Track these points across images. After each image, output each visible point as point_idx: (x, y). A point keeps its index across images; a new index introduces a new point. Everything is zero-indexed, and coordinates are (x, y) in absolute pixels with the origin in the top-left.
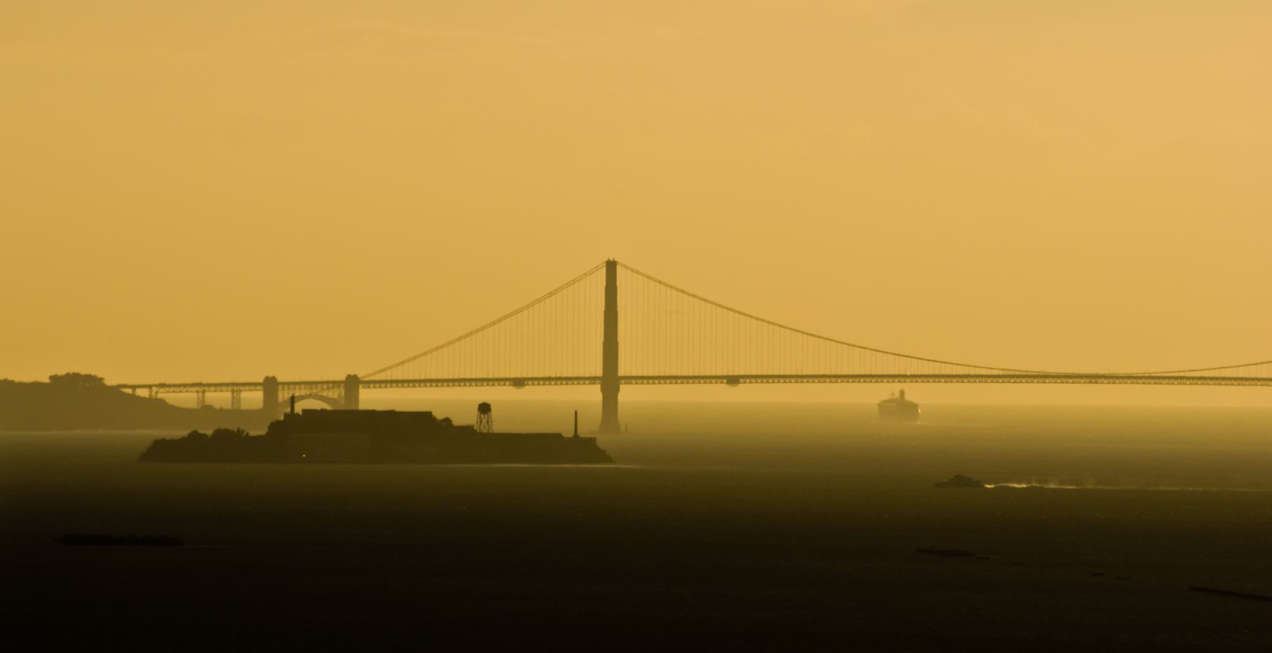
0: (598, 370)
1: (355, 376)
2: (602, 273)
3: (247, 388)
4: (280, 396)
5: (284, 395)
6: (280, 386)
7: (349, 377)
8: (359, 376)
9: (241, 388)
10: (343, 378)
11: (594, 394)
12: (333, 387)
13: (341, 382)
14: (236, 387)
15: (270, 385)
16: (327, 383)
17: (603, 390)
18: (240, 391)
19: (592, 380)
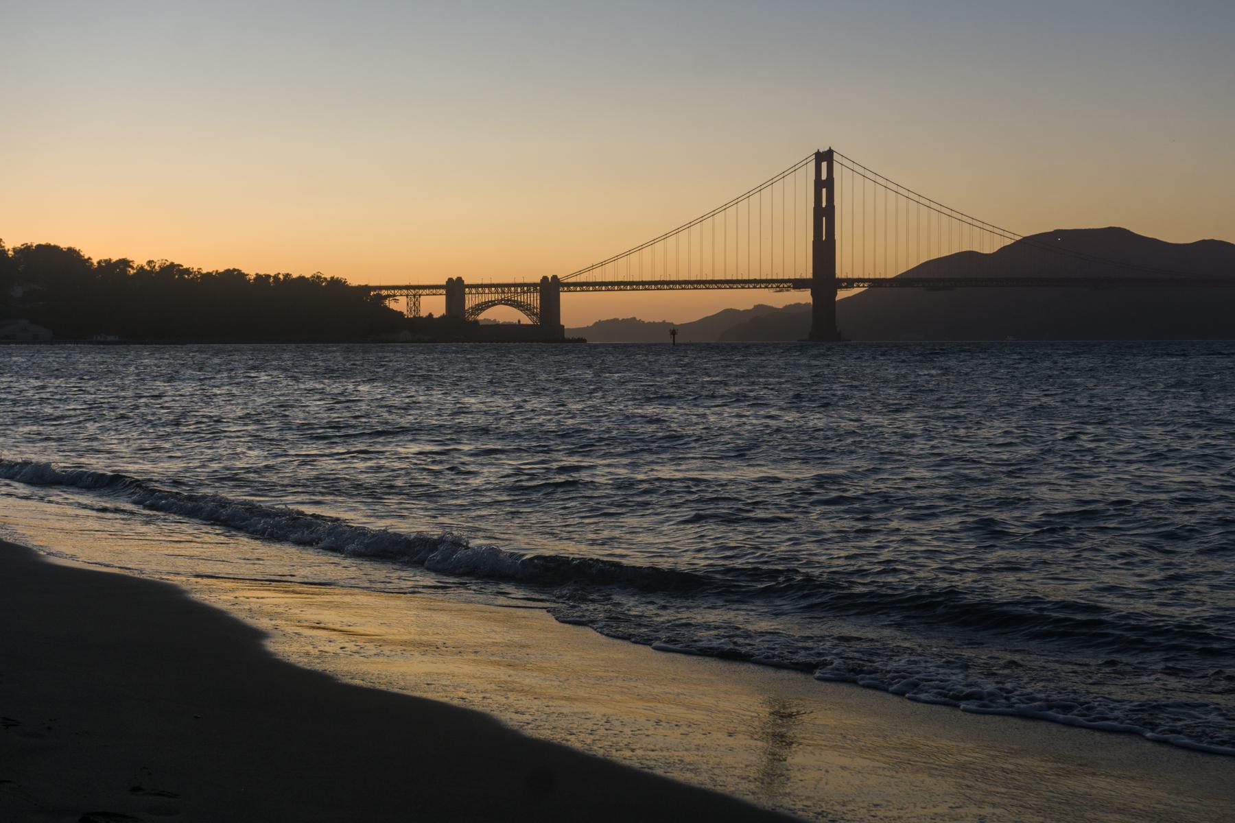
0: (809, 274)
1: (555, 277)
2: (812, 165)
3: (427, 291)
4: (467, 302)
5: (471, 301)
6: (467, 290)
7: (545, 278)
8: (559, 277)
9: (421, 292)
10: (538, 280)
11: (804, 297)
12: (529, 291)
13: (534, 285)
14: (414, 290)
15: (455, 289)
16: (522, 285)
17: (812, 294)
18: (420, 295)
19: (798, 284)
